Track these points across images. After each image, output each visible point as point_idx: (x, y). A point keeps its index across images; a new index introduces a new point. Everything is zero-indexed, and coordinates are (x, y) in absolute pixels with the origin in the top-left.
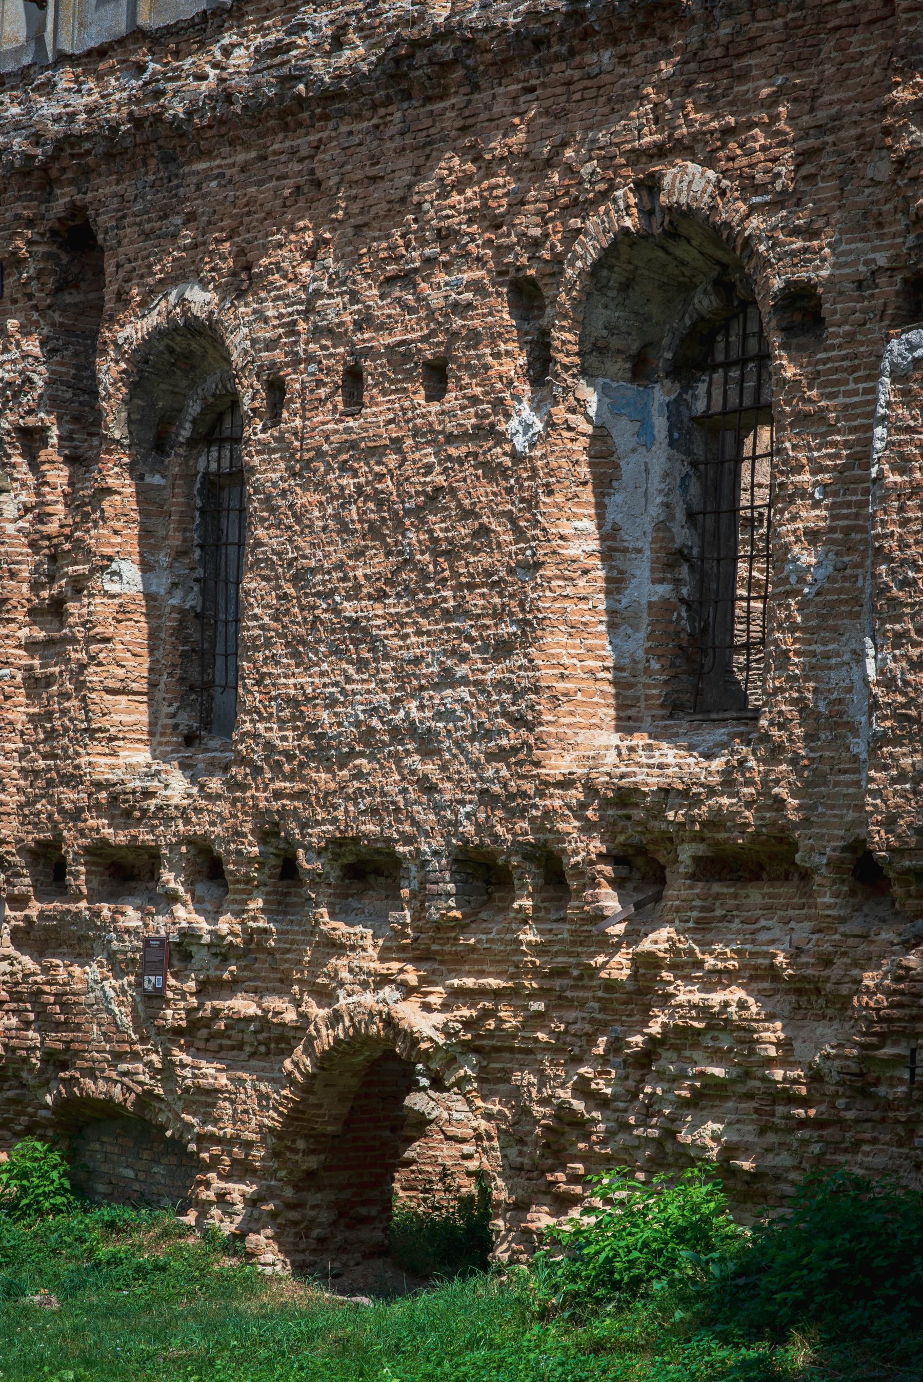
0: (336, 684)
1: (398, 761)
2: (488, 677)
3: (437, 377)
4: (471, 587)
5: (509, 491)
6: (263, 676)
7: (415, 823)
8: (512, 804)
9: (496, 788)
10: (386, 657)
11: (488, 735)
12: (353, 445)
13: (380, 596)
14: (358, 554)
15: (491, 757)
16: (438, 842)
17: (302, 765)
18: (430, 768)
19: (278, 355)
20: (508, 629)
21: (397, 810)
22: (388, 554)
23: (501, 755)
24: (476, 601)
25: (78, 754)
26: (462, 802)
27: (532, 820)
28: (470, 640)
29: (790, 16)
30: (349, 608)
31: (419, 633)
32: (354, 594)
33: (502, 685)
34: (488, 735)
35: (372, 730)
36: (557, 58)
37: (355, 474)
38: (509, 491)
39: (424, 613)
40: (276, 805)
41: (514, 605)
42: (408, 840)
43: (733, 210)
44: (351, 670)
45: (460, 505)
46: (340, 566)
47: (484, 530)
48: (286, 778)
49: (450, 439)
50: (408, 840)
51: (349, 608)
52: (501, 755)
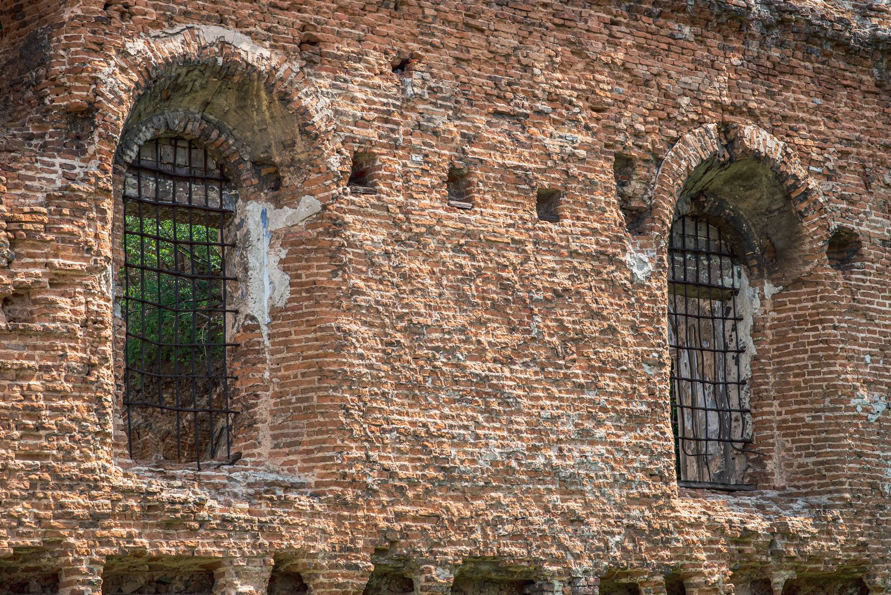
0: (466, 428)
1: (538, 499)
2: (624, 440)
3: (548, 204)
4: (602, 370)
5: (630, 306)
6: (371, 410)
7: (561, 546)
8: (658, 537)
9: (643, 525)
10: (519, 412)
11: (628, 483)
12: (469, 234)
13: (508, 361)
14: (480, 323)
15: (632, 500)
16: (587, 564)
17: (427, 491)
18: (575, 505)
19: (372, 133)
20: (639, 407)
21: (544, 537)
22: (512, 330)
23: (644, 499)
24: (605, 381)
25: (88, 458)
26: (612, 534)
27: (675, 549)
28: (604, 410)
29: (817, 65)
30: (475, 367)
31: (551, 397)
32: (479, 354)
33: (638, 449)
34: (628, 483)
35: (509, 470)
36: (650, 14)
37: (473, 257)
38: (630, 306)
39: (556, 382)
40: (397, 526)
41: (642, 390)
42: (555, 561)
43: (797, 169)
44: (481, 418)
45: (587, 306)
46: (463, 330)
47: (613, 330)
48: (408, 502)
49: (573, 254)
50: (555, 561)
51: (475, 367)
52: (644, 499)
